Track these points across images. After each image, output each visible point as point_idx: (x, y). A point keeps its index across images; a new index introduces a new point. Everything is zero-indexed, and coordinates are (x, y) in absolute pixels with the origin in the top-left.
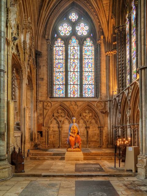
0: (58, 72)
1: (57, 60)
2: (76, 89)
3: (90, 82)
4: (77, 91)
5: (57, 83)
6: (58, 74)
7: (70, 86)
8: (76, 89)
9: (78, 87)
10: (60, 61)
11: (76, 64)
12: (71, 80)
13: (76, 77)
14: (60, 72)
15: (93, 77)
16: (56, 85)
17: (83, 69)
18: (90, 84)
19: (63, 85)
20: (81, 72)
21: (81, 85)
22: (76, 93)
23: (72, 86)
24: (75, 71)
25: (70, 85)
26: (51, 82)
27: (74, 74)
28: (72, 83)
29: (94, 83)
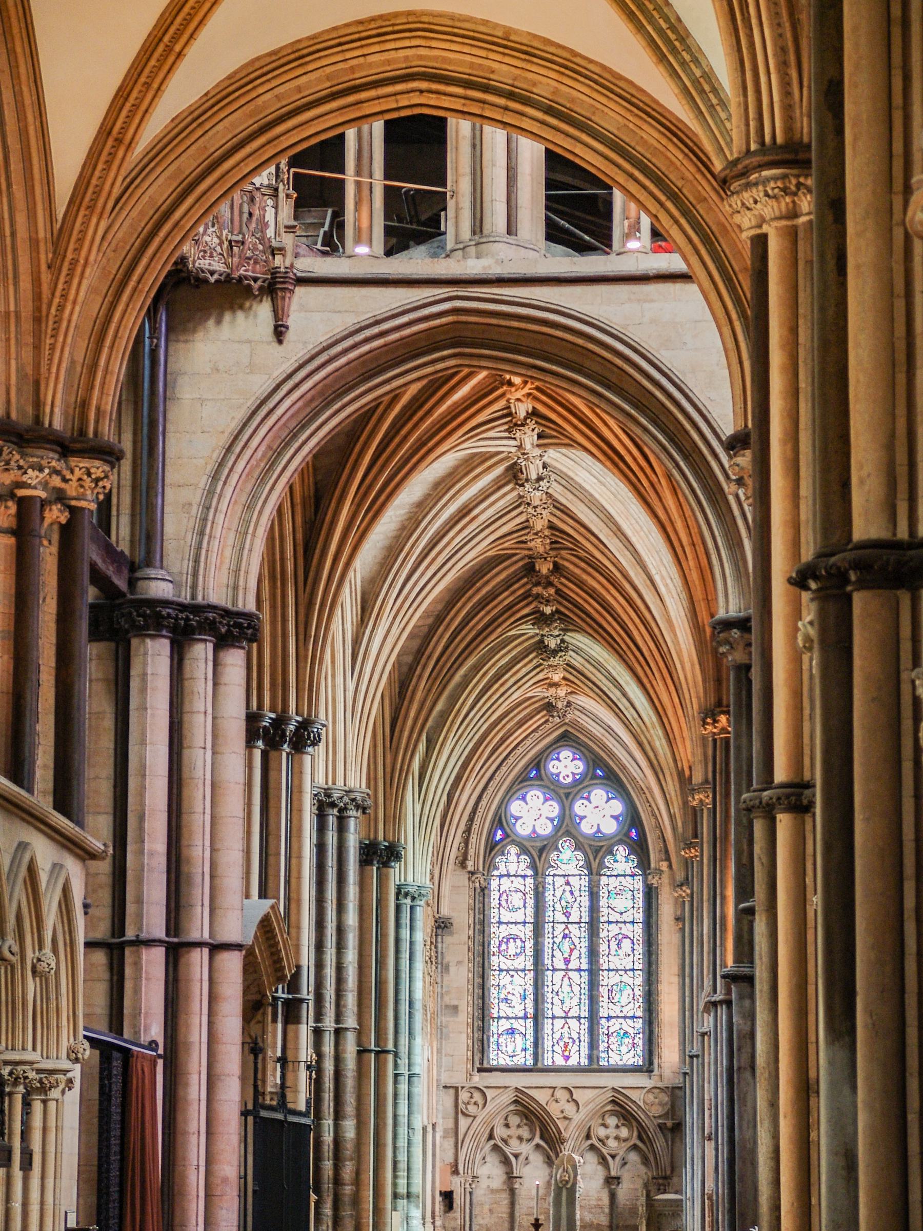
0: (507, 971)
1: (503, 927)
2: (575, 1036)
3: (624, 1009)
4: (580, 1041)
5: (502, 1014)
6: (508, 978)
7: (553, 1024)
8: (575, 1036)
9: (582, 1027)
10: (514, 930)
11: (576, 941)
12: (556, 1001)
13: (576, 989)
14: (516, 970)
15: (636, 989)
16: (499, 1018)
17: (601, 961)
18: (625, 1017)
19: (525, 1017)
20: (593, 972)
21: (593, 1018)
22: (576, 1048)
23: (559, 1023)
24: (570, 967)
25: (553, 1018)
26: (483, 1009)
27: (566, 979)
28: (558, 1012)
29: (644, 1011)
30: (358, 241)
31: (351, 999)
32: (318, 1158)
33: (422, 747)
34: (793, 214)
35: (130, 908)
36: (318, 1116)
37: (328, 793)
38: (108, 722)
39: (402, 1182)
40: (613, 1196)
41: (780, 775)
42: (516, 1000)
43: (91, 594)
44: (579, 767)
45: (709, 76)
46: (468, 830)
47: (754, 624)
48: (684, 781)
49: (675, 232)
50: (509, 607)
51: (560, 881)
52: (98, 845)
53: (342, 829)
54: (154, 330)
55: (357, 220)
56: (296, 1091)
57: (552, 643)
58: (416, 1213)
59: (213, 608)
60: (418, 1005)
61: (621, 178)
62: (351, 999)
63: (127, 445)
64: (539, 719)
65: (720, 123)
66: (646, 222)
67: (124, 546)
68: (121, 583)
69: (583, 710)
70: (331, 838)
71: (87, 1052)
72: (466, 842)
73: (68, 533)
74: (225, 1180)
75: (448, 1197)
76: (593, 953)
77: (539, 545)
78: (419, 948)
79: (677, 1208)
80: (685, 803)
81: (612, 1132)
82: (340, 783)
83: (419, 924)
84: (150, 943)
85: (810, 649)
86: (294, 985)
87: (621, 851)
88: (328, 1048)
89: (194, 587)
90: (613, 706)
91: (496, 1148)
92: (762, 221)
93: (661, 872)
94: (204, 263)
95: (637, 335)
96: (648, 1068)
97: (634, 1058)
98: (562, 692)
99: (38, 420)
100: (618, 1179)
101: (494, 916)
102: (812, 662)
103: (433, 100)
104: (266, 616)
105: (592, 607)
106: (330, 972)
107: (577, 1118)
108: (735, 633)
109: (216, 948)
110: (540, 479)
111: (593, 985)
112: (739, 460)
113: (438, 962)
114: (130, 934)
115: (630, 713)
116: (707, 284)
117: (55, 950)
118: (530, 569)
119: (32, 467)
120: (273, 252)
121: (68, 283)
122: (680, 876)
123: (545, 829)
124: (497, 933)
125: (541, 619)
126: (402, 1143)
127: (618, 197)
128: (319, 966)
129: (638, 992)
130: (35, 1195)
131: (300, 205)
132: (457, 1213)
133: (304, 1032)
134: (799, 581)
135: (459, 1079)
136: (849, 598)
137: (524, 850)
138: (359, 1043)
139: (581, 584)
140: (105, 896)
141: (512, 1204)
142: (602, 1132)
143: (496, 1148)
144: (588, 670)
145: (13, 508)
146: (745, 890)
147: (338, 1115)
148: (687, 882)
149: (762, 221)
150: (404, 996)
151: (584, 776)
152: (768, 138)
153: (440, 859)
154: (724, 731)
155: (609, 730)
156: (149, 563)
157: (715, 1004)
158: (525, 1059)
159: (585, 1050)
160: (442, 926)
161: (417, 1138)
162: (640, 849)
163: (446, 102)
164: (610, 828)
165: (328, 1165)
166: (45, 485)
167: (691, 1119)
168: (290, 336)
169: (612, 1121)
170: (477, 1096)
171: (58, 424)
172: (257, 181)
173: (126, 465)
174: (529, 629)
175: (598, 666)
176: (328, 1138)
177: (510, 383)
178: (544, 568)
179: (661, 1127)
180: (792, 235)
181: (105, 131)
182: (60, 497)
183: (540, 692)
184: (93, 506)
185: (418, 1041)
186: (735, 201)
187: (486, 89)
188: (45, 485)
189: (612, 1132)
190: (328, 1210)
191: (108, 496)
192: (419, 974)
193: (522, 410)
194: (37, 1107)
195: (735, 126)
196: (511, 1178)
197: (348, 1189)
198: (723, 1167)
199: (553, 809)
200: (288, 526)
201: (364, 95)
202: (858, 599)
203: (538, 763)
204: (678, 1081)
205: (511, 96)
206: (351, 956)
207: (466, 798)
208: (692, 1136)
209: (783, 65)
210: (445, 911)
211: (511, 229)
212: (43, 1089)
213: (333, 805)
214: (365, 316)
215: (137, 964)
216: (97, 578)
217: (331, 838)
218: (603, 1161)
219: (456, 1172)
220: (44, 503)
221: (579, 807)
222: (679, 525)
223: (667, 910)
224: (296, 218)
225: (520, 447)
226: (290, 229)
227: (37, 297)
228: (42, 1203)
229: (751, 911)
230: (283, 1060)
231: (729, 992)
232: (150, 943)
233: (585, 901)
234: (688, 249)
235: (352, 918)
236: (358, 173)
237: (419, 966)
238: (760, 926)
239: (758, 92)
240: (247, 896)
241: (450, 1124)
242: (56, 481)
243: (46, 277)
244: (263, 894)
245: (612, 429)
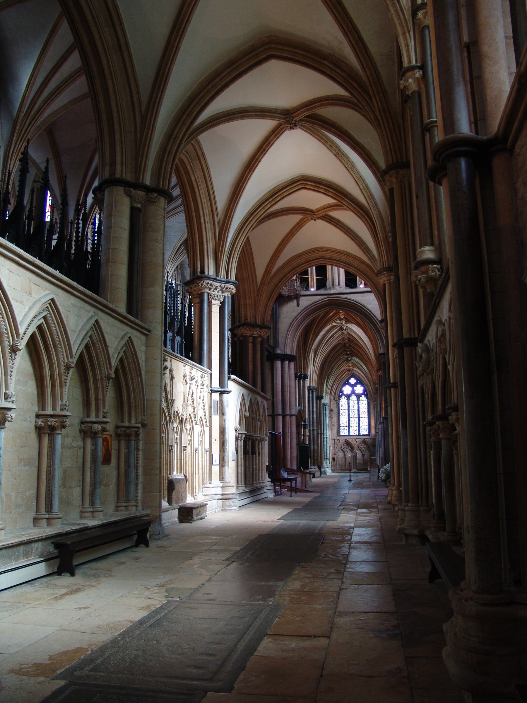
21: (359, 426)
30: (311, 287)
31: (315, 424)
32: (310, 452)
33: (326, 378)
34: (390, 280)
35: (275, 409)
36: (310, 445)
37: (310, 387)
38: (270, 376)
39: (326, 456)
40: (363, 458)
41: (391, 381)
42: (345, 423)
43: (266, 353)
45: (373, 256)
46: (335, 393)
47: (386, 354)
48: (374, 383)
49: (369, 284)
50: (341, 353)
51: (352, 402)
52: (269, 398)
53: (312, 394)
54: (276, 306)
55: (311, 284)
56: (306, 441)
57: (349, 359)
58: (328, 462)
59: (288, 355)
60: (327, 425)
61: (358, 275)
62: (315, 424)
63: (272, 326)
64: (347, 373)
65: (376, 264)
66: (363, 282)
67: (272, 345)
68: (271, 351)
69: (355, 371)
70: (311, 395)
71: (269, 434)
72: (335, 395)
73: (262, 343)
74: (294, 456)
75: (334, 459)
76: (359, 415)
77: (346, 341)
78: (327, 414)
79: (375, 460)
80: (374, 387)
81: (363, 446)
82: (312, 385)
83: (327, 410)
84: (279, 415)
85: (396, 358)
86: (305, 422)
87: (363, 396)
88: (311, 433)
89: (284, 351)
90: (360, 370)
91: (342, 450)
92: (384, 281)
93: (370, 400)
94: (283, 293)
95: (362, 303)
96: (369, 435)
97: (367, 433)
98: (351, 368)
99: (256, 323)
100: (364, 455)
101: (340, 408)
102: (397, 360)
103: (324, 262)
104: (297, 356)
105: (356, 352)
106: (311, 419)
107: (357, 444)
108: (382, 356)
109: (291, 415)
110: (346, 329)
111: (359, 420)
112: (382, 324)
113: (331, 417)
114: (275, 413)
115: (364, 371)
116: (375, 293)
117: (262, 417)
118: (345, 345)
119: (255, 331)
120: (296, 291)
121: (260, 298)
122: (374, 400)
124: (341, 411)
125: (347, 355)
126: (325, 449)
127: (358, 277)
128: (309, 418)
129: (367, 421)
130: (261, 460)
131: (301, 282)
132: (336, 461)
133: (307, 430)
134: (394, 346)
135: (335, 438)
136: (403, 349)
137: (345, 396)
138: (317, 432)
139: (354, 348)
140: (271, 407)
141: (345, 459)
142: (361, 446)
143: (342, 450)
144: (356, 363)
145: (252, 338)
146: (386, 402)
147: (314, 445)
148: (375, 401)
149: (384, 281)
150: (325, 423)
151: (356, 383)
152: (385, 266)
153: (330, 398)
154: (381, 373)
155: (360, 374)
156: (276, 347)
157: (381, 423)
159: (358, 432)
160: (331, 410)
161: (328, 448)
162: (366, 395)
163: (326, 263)
164: (361, 392)
165: (312, 454)
166: (257, 334)
167: (377, 443)
168: (300, 305)
169: (363, 444)
170: (338, 441)
171: (259, 323)
172: (293, 278)
173: (272, 330)
174: (345, 357)
175: (358, 363)
176: (312, 448)
177: (340, 312)
178: (347, 345)
179: (372, 445)
180: (390, 283)
181: (266, 271)
182: (260, 336)
183: (347, 368)
184: (266, 337)
185: (327, 431)
186: (380, 278)
187: (333, 260)
188: (257, 334)
189: (363, 446)
190: (312, 461)
191: (269, 336)
192: (327, 419)
193: (342, 317)
194: (260, 444)
195: (379, 264)
196: (345, 455)
197: (316, 458)
198: (383, 452)
199: (351, 389)
200: (301, 340)
201: (312, 262)
202: (405, 349)
203: (348, 380)
204: (375, 437)
205: (338, 261)
206: (315, 416)
207: (335, 387)
208: (377, 447)
209: (387, 253)
210: (332, 408)
211: (339, 285)
212: (261, 441)
213: (311, 389)
214: (313, 301)
215: (277, 419)
216: (267, 350)
217: (311, 395)
218: (361, 452)
219: (335, 454)
220: (257, 337)
221: (355, 388)
222: (371, 336)
223: (372, 407)
224: (300, 284)
225: (342, 324)
226: (299, 286)
227: (255, 301)
228: (262, 461)
229: (387, 406)
230: (303, 435)
231: (383, 421)
232: (279, 415)
233: (357, 405)
234: (371, 287)
235: (315, 410)
236: (311, 276)
237: (327, 418)
238: (389, 409)
239: (382, 258)
240: (296, 406)
241: (334, 446)
242: (259, 333)
243: (256, 297)
244: (299, 406)
245: (359, 320)
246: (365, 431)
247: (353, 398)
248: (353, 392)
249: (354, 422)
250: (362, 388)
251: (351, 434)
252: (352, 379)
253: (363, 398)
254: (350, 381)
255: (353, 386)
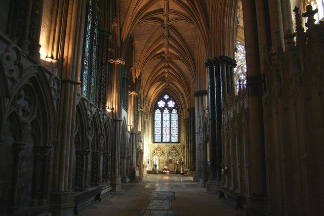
44: (168, 97)
87: (174, 110)
96: (178, 142)
123: (163, 106)
158: (160, 141)
164: (173, 106)
199: (164, 103)
221: (168, 103)
246: (174, 139)
247: (166, 111)
248: (166, 106)
249: (166, 124)
250: (174, 103)
251: (164, 141)
252: (166, 96)
253: (174, 111)
254: (164, 97)
255: (166, 101)
